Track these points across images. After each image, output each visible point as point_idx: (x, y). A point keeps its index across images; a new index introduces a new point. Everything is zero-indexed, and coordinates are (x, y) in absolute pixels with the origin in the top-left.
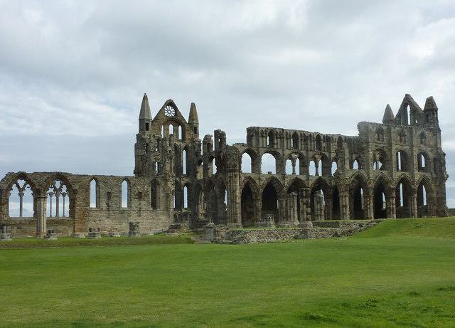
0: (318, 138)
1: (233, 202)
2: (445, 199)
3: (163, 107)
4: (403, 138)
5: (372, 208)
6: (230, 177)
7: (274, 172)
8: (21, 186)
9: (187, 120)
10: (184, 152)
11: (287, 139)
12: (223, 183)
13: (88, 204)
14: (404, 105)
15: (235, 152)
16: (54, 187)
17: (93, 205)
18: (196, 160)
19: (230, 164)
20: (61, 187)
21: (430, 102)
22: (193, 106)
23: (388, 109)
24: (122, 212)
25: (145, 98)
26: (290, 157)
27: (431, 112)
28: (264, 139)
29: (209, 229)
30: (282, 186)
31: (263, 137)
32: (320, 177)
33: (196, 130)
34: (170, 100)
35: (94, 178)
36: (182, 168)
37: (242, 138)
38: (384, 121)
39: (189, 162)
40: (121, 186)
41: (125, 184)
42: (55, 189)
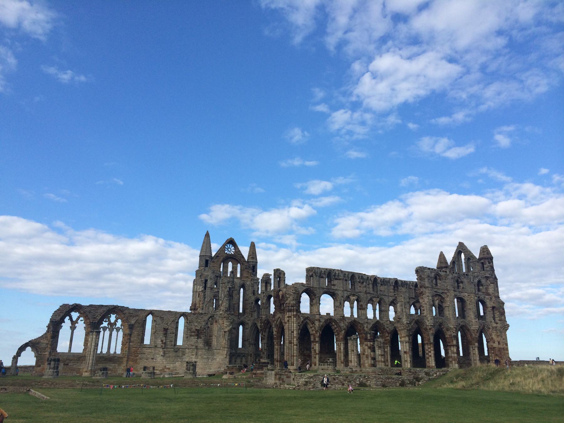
0: (375, 280)
2: (507, 349)
3: (224, 246)
4: (461, 285)
5: (433, 355)
6: (289, 317)
8: (74, 319)
9: (246, 257)
12: (281, 323)
13: (142, 340)
14: (458, 253)
15: (298, 290)
16: (109, 321)
17: (147, 341)
18: (253, 298)
20: (116, 321)
21: (485, 250)
23: (442, 256)
24: (177, 349)
25: (207, 235)
27: (487, 261)
29: (270, 372)
31: (323, 277)
32: (378, 321)
34: (231, 238)
35: (151, 312)
38: (437, 268)
40: (178, 322)
41: (182, 321)
42: (110, 324)
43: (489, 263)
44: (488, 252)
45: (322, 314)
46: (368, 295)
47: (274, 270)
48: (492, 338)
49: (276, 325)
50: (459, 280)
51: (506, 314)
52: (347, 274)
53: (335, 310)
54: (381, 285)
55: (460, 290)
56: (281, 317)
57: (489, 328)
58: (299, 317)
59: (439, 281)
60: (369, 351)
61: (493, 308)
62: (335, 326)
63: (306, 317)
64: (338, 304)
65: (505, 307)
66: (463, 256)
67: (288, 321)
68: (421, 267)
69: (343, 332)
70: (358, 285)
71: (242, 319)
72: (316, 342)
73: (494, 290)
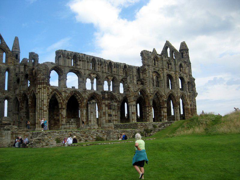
1: (42, 110)
2: (196, 109)
4: (170, 66)
6: (40, 89)
7: (77, 87)
10: (7, 73)
11: (88, 62)
15: (47, 69)
19: (40, 78)
21: (183, 45)
22: (16, 39)
26: (89, 76)
27: (185, 52)
28: (70, 60)
29: (6, 132)
30: (83, 99)
31: (69, 58)
33: (17, 57)
36: (4, 85)
37: (52, 59)
39: (10, 81)
43: (186, 53)
44: (186, 46)
45: (68, 87)
46: (104, 74)
47: (30, 53)
48: (187, 102)
49: (30, 97)
50: (169, 63)
51: (196, 87)
52: (89, 57)
53: (79, 85)
54: (115, 67)
55: (170, 69)
56: (34, 90)
57: (186, 96)
58: (48, 89)
59: (156, 62)
60: (107, 108)
61: (188, 82)
62: (79, 97)
63: (55, 89)
64: (81, 80)
65: (195, 82)
66: (168, 50)
67: (39, 92)
68: (145, 51)
69: (85, 101)
70: (97, 66)
71: (7, 94)
72: (63, 109)
73: (189, 71)
